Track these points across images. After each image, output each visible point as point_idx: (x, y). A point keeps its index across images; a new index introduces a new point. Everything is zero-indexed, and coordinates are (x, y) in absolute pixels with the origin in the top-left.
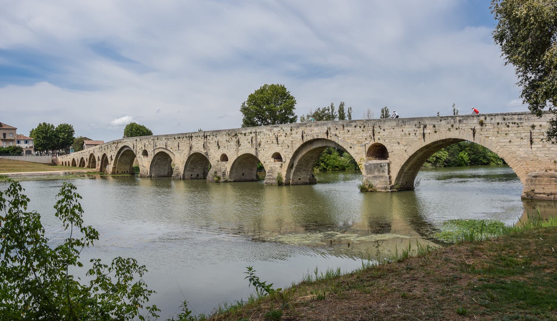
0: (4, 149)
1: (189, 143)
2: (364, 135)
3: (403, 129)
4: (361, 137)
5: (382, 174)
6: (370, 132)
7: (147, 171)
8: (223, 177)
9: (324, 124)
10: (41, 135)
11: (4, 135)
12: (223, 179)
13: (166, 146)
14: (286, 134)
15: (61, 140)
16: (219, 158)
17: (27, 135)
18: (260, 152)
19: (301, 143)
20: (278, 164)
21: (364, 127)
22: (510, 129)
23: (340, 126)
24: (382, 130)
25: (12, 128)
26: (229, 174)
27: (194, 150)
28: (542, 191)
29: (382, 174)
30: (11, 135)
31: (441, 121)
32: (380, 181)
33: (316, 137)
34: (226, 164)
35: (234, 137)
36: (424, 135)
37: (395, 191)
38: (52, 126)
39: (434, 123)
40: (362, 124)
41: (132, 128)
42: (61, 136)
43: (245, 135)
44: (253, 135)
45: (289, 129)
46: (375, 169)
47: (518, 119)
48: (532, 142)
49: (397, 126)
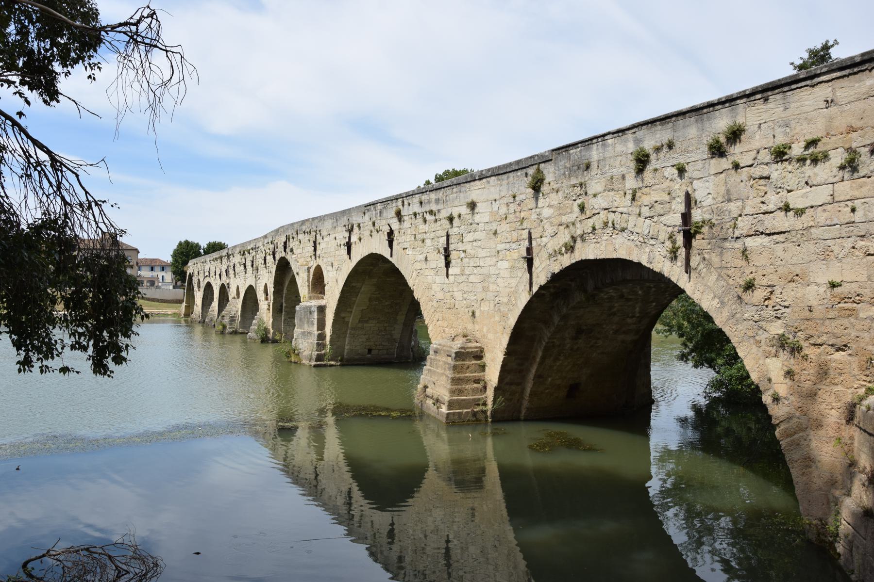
8: (231, 324)
10: (180, 258)
12: (230, 328)
13: (209, 273)
25: (130, 248)
37: (331, 366)
38: (198, 246)
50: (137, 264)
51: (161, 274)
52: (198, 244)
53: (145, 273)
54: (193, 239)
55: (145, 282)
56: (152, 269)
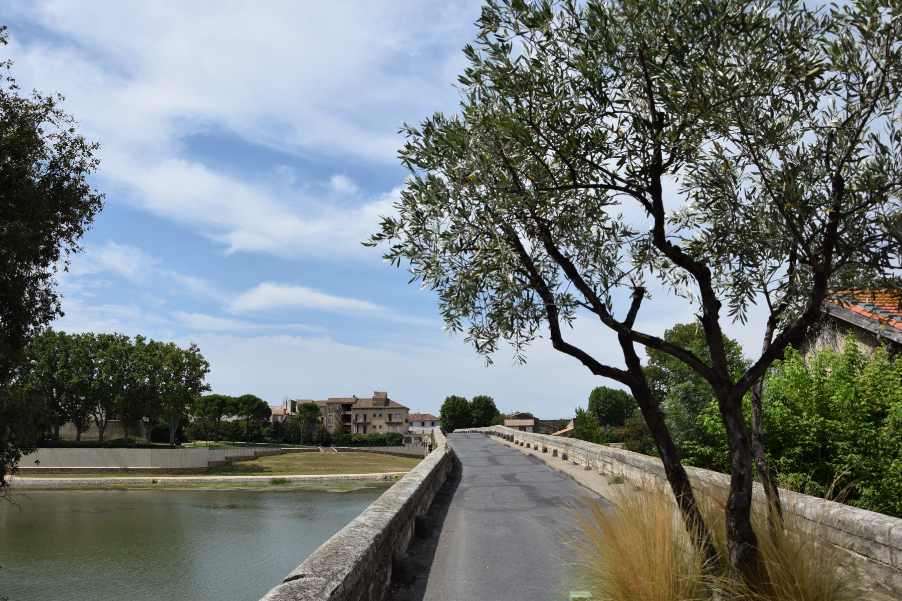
0: (379, 437)
11: (390, 416)
15: (475, 420)
17: (438, 415)
30: (398, 416)
38: (464, 401)
41: (599, 396)
42: (474, 415)
50: (407, 421)
51: (428, 430)
52: (464, 398)
53: (416, 429)
54: (459, 395)
55: (413, 439)
56: (423, 424)
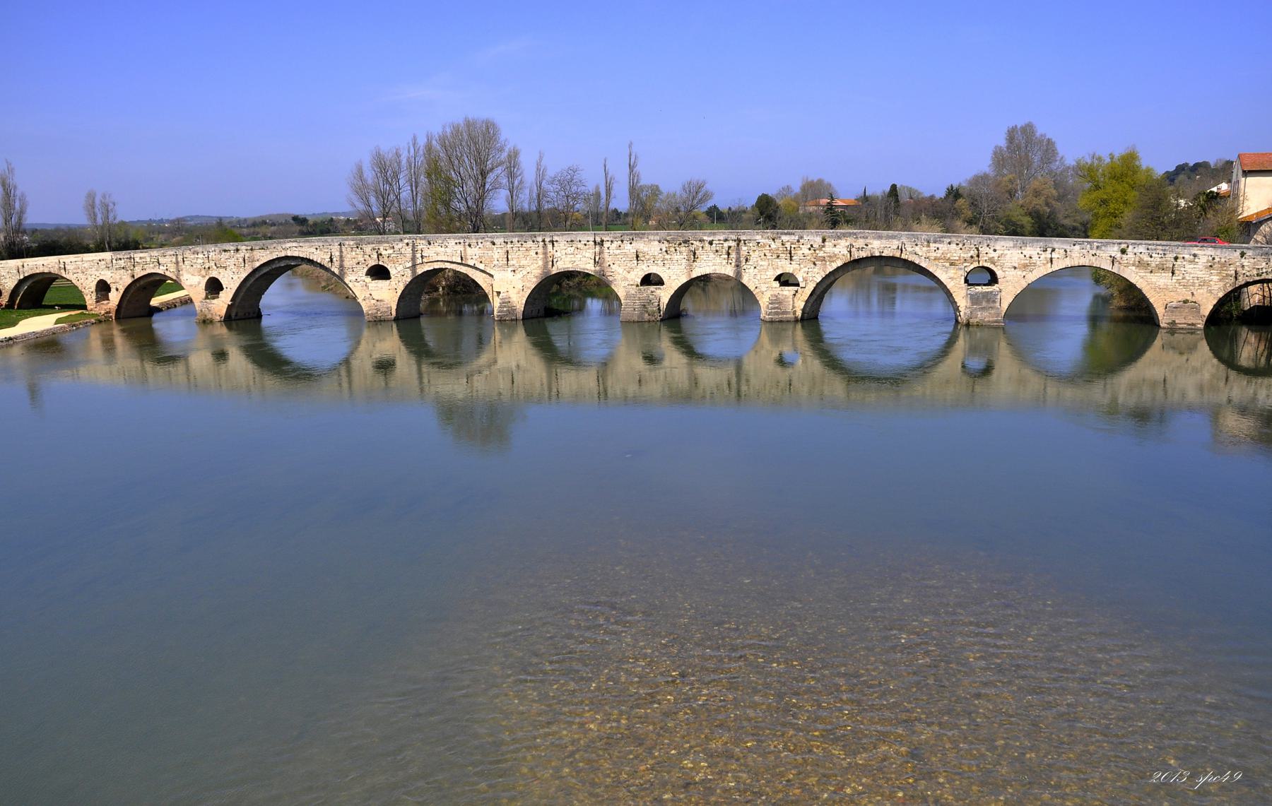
1: (545, 254)
2: (962, 255)
3: (1023, 252)
4: (957, 258)
5: (992, 305)
6: (974, 252)
7: (388, 308)
9: (893, 237)
13: (462, 258)
14: (812, 246)
16: (639, 281)
18: (747, 271)
19: (848, 259)
20: (788, 291)
21: (964, 245)
22: (1152, 259)
23: (923, 241)
24: (991, 251)
26: (665, 307)
27: (560, 267)
28: (1184, 321)
29: (992, 305)
31: (1074, 245)
32: (990, 313)
33: (877, 254)
34: (658, 291)
35: (683, 245)
36: (1051, 259)
39: (1065, 247)
40: (960, 241)
43: (711, 243)
44: (733, 244)
45: (819, 240)
46: (983, 298)
47: (1162, 250)
48: (1173, 273)
49: (1014, 247)
